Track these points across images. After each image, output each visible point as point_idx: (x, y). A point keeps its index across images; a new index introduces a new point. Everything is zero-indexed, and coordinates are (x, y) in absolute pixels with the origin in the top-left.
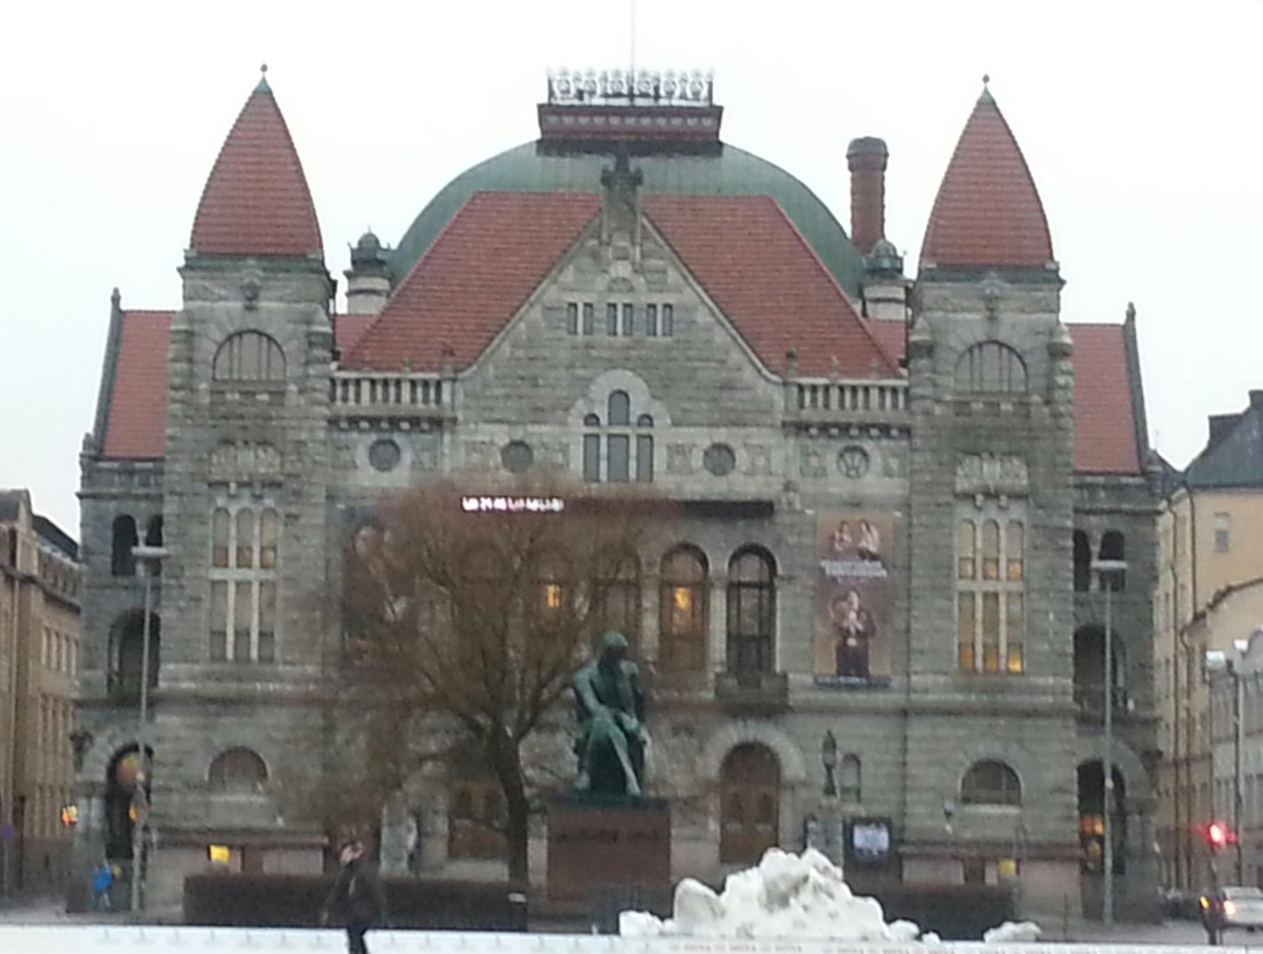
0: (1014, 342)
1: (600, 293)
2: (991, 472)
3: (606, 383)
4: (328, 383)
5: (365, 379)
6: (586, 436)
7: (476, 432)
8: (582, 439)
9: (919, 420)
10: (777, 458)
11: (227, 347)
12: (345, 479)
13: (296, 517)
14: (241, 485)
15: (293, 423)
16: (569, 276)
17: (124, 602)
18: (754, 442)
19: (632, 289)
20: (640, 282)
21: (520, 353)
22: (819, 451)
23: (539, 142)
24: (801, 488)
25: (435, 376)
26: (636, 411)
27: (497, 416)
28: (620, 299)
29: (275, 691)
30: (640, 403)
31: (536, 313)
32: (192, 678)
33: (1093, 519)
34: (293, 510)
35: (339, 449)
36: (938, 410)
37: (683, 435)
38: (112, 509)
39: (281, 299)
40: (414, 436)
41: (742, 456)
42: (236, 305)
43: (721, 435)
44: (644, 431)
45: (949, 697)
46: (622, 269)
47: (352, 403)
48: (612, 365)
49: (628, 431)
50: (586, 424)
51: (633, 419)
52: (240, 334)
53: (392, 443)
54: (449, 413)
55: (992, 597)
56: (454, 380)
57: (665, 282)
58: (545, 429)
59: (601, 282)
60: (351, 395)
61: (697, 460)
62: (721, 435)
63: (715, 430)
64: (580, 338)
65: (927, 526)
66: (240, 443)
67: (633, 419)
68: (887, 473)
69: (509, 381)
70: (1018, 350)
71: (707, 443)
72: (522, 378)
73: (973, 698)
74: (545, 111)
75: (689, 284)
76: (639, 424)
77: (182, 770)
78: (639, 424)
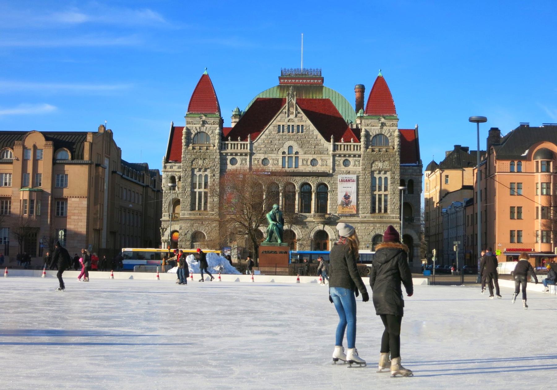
0: (386, 134)
1: (286, 122)
4: (221, 144)
7: (256, 156)
8: (282, 157)
11: (197, 135)
15: (212, 154)
16: (279, 118)
17: (174, 196)
20: (296, 119)
22: (339, 160)
23: (278, 86)
26: (294, 151)
27: (261, 152)
31: (271, 127)
33: (407, 177)
35: (223, 160)
37: (306, 157)
41: (320, 162)
43: (315, 156)
44: (296, 156)
45: (370, 219)
48: (289, 139)
49: (293, 155)
50: (283, 154)
51: (294, 153)
52: (200, 132)
55: (380, 195)
58: (272, 155)
61: (309, 163)
62: (315, 156)
63: (314, 155)
64: (281, 133)
71: (311, 158)
73: (376, 219)
74: (280, 78)
76: (295, 154)
78: (295, 154)
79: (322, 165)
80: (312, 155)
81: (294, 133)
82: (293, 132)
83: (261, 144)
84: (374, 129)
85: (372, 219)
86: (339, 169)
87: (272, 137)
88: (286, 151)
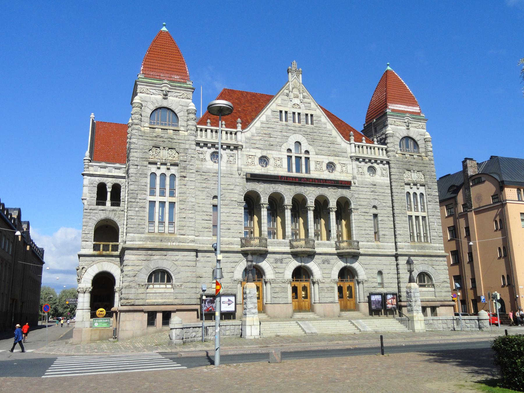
1: (290, 108)
2: (415, 177)
3: (294, 138)
5: (210, 129)
6: (288, 156)
7: (250, 151)
9: (392, 158)
10: (349, 167)
12: (202, 165)
13: (185, 177)
14: (162, 164)
15: (183, 142)
17: (102, 216)
20: (302, 106)
21: (264, 125)
24: (357, 178)
26: (304, 148)
27: (257, 146)
28: (297, 111)
29: (176, 245)
30: (305, 146)
32: (141, 240)
34: (184, 174)
36: (397, 155)
37: (320, 158)
38: (98, 180)
41: (338, 167)
42: (160, 97)
43: (331, 159)
45: (409, 250)
46: (296, 101)
47: (204, 137)
48: (295, 132)
51: (303, 151)
54: (240, 143)
56: (242, 132)
57: (310, 107)
58: (273, 152)
59: (290, 104)
65: (398, 193)
66: (161, 148)
68: (383, 175)
69: (261, 135)
70: (416, 139)
71: (327, 162)
72: (265, 134)
77: (136, 278)
79: (342, 172)
80: (327, 157)
81: (302, 123)
82: (299, 122)
83: (256, 135)
84: (401, 130)
85: (412, 250)
86: (363, 179)
88: (293, 148)
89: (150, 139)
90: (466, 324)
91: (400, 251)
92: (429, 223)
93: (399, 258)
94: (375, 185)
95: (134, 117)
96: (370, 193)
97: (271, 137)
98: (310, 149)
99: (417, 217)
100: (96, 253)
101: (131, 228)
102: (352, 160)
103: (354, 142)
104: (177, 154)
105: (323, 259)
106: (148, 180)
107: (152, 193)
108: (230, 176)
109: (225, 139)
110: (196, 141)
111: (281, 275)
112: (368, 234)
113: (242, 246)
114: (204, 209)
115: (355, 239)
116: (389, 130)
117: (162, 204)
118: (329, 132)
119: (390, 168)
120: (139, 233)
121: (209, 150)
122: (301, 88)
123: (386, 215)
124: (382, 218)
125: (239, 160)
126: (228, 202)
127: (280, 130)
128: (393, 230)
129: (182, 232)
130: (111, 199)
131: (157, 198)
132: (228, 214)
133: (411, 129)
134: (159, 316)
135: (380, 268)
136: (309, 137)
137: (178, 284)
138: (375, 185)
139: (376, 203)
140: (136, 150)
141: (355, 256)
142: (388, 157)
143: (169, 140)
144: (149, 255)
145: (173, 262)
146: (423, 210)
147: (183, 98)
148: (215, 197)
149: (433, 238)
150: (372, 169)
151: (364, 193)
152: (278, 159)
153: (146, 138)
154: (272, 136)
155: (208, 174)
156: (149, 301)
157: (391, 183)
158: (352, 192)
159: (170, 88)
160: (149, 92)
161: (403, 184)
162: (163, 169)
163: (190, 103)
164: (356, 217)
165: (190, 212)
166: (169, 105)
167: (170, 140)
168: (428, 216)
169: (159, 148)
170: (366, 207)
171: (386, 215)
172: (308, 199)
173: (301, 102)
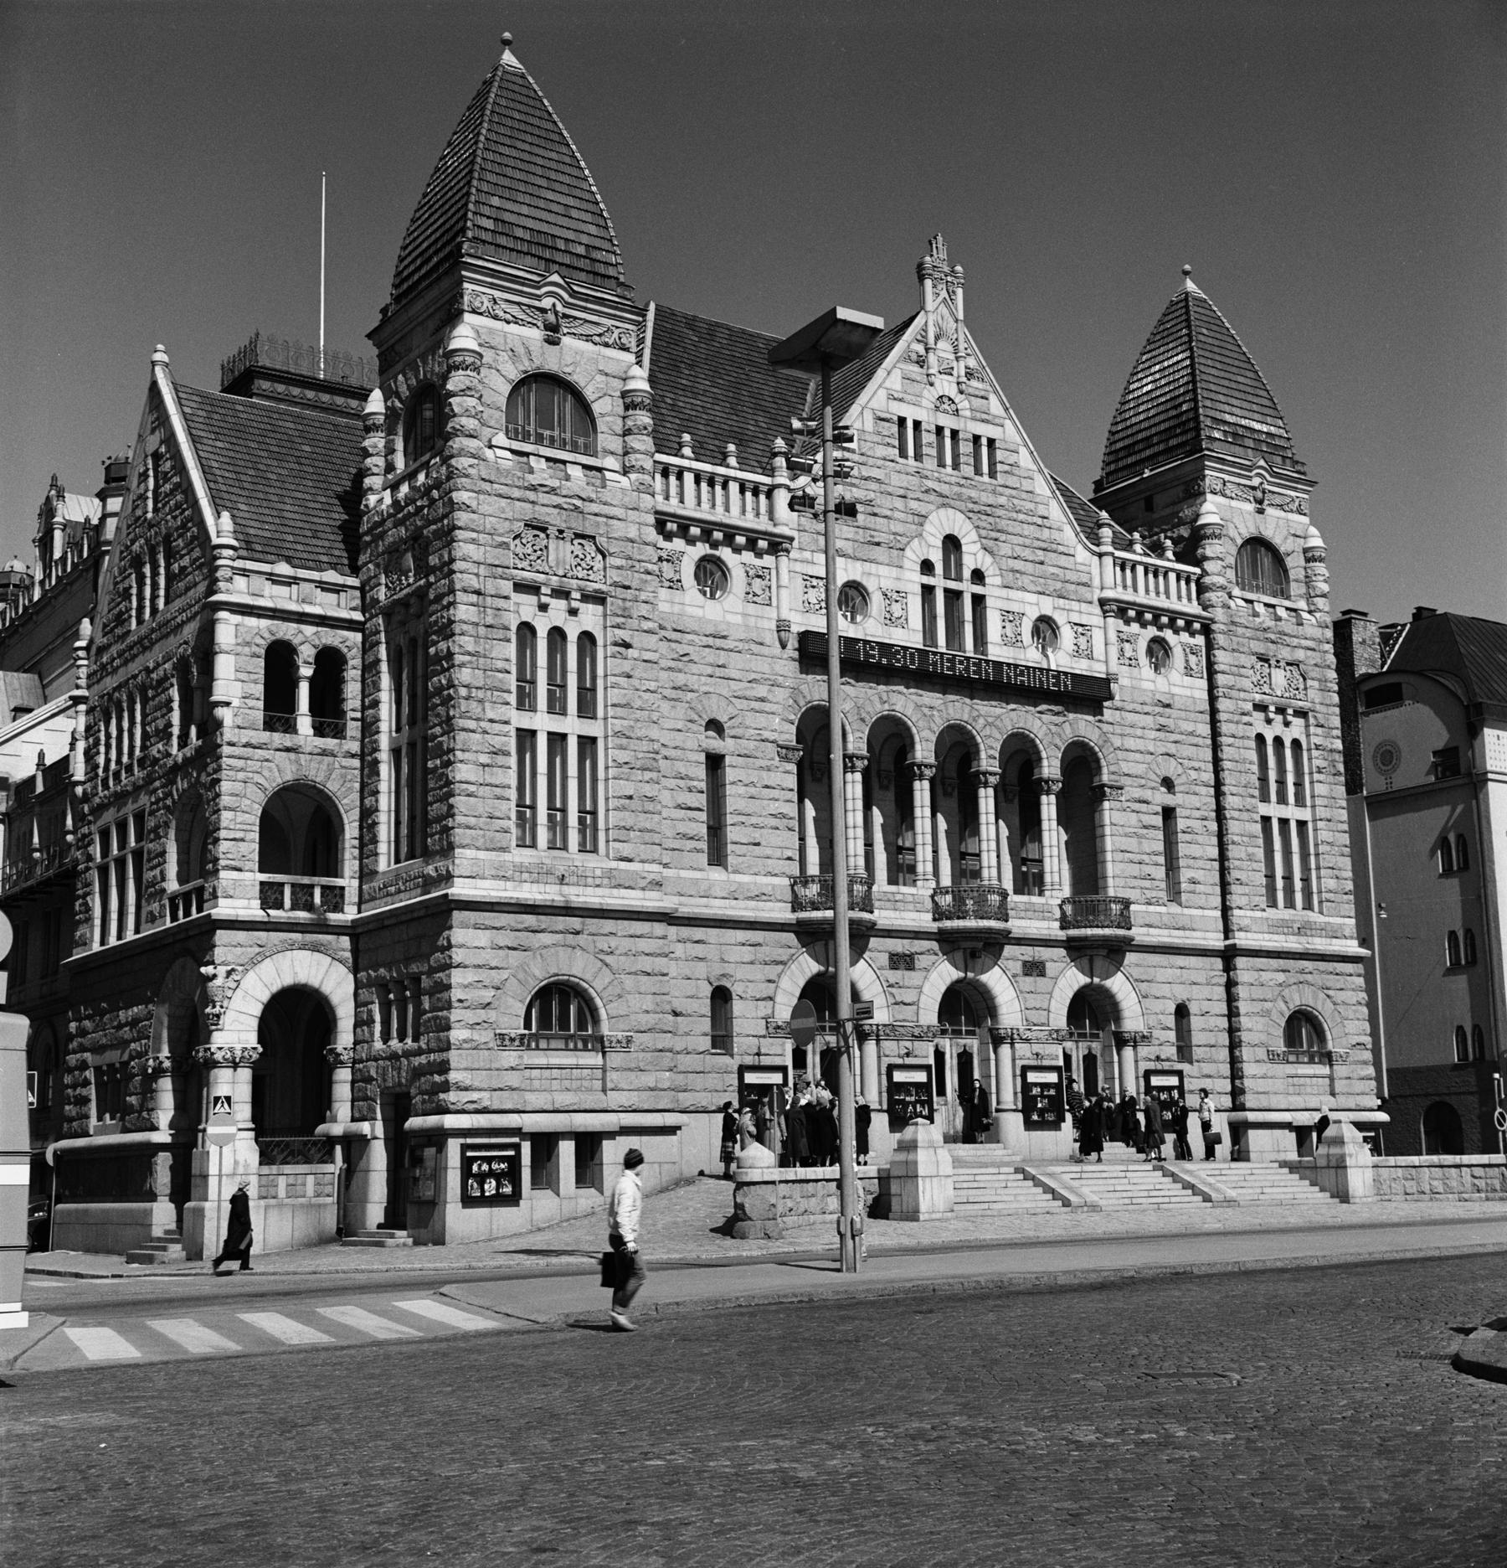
13: (627, 646)
18: (1076, 618)
19: (956, 412)
25: (767, 480)
26: (969, 563)
28: (948, 422)
30: (973, 556)
34: (623, 634)
39: (588, 338)
40: (748, 557)
41: (1067, 635)
42: (536, 334)
43: (1047, 606)
44: (978, 590)
48: (945, 501)
51: (967, 574)
53: (718, 562)
60: (673, 490)
66: (552, 531)
67: (967, 574)
70: (1282, 550)
75: (1011, 418)
77: (491, 1015)
80: (1033, 598)
87: (875, 473)
88: (936, 557)
89: (517, 493)
90: (1476, 1181)
91: (1242, 940)
92: (1316, 845)
93: (1240, 962)
94: (1168, 706)
95: (460, 405)
96: (1154, 734)
97: (875, 515)
98: (986, 563)
99: (1284, 822)
100: (302, 915)
101: (470, 828)
102: (1104, 612)
103: (1110, 549)
104: (600, 557)
105: (1026, 958)
106: (511, 650)
107: (525, 701)
108: (755, 648)
109: (738, 512)
110: (657, 512)
111: (908, 1013)
112: (1149, 877)
113: (797, 905)
114: (682, 768)
115: (1111, 892)
116: (1211, 510)
117: (557, 740)
118: (1042, 510)
119: (1210, 646)
120: (494, 849)
121: (690, 549)
122: (962, 338)
123: (1197, 814)
124: (1189, 823)
125: (783, 592)
126: (752, 744)
127: (902, 492)
128: (1216, 865)
129: (626, 849)
130: (314, 710)
131: (542, 722)
132: (752, 791)
133: (1270, 511)
134: (567, 1151)
135: (1181, 993)
136: (985, 521)
137: (620, 1035)
138: (1168, 706)
139: (1171, 769)
140: (474, 535)
141: (1114, 951)
142: (1205, 609)
143: (576, 502)
144: (527, 930)
145: (602, 956)
146: (1300, 801)
147: (606, 345)
148: (714, 726)
149: (1330, 896)
150: (1159, 651)
151: (1139, 732)
152: (895, 596)
153: (504, 490)
154: (876, 510)
155: (689, 637)
156: (535, 1100)
157: (1212, 699)
158: (1105, 727)
159: (567, 305)
160: (501, 314)
161: (1249, 707)
162: (558, 611)
163: (630, 367)
164: (1118, 817)
165: (648, 775)
166: (567, 370)
167: (578, 503)
168: (1314, 821)
169: (544, 530)
170: (1143, 782)
171: (1197, 814)
172: (982, 747)
173: (961, 392)
